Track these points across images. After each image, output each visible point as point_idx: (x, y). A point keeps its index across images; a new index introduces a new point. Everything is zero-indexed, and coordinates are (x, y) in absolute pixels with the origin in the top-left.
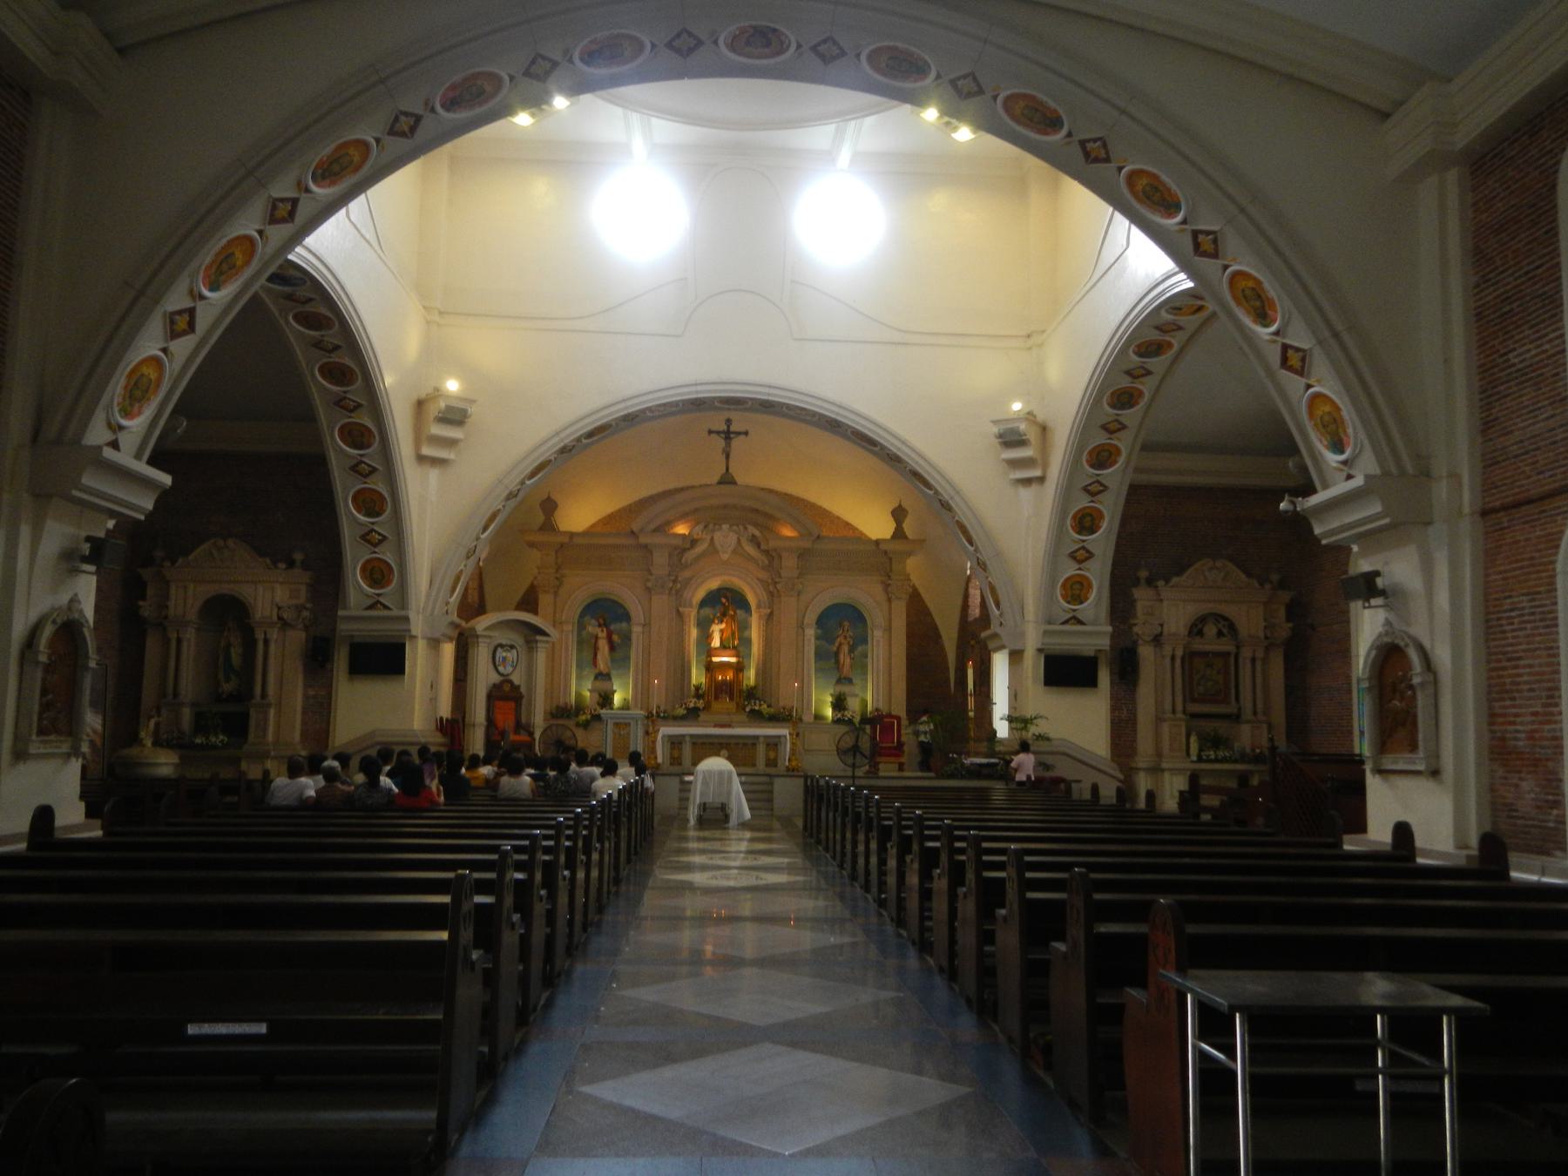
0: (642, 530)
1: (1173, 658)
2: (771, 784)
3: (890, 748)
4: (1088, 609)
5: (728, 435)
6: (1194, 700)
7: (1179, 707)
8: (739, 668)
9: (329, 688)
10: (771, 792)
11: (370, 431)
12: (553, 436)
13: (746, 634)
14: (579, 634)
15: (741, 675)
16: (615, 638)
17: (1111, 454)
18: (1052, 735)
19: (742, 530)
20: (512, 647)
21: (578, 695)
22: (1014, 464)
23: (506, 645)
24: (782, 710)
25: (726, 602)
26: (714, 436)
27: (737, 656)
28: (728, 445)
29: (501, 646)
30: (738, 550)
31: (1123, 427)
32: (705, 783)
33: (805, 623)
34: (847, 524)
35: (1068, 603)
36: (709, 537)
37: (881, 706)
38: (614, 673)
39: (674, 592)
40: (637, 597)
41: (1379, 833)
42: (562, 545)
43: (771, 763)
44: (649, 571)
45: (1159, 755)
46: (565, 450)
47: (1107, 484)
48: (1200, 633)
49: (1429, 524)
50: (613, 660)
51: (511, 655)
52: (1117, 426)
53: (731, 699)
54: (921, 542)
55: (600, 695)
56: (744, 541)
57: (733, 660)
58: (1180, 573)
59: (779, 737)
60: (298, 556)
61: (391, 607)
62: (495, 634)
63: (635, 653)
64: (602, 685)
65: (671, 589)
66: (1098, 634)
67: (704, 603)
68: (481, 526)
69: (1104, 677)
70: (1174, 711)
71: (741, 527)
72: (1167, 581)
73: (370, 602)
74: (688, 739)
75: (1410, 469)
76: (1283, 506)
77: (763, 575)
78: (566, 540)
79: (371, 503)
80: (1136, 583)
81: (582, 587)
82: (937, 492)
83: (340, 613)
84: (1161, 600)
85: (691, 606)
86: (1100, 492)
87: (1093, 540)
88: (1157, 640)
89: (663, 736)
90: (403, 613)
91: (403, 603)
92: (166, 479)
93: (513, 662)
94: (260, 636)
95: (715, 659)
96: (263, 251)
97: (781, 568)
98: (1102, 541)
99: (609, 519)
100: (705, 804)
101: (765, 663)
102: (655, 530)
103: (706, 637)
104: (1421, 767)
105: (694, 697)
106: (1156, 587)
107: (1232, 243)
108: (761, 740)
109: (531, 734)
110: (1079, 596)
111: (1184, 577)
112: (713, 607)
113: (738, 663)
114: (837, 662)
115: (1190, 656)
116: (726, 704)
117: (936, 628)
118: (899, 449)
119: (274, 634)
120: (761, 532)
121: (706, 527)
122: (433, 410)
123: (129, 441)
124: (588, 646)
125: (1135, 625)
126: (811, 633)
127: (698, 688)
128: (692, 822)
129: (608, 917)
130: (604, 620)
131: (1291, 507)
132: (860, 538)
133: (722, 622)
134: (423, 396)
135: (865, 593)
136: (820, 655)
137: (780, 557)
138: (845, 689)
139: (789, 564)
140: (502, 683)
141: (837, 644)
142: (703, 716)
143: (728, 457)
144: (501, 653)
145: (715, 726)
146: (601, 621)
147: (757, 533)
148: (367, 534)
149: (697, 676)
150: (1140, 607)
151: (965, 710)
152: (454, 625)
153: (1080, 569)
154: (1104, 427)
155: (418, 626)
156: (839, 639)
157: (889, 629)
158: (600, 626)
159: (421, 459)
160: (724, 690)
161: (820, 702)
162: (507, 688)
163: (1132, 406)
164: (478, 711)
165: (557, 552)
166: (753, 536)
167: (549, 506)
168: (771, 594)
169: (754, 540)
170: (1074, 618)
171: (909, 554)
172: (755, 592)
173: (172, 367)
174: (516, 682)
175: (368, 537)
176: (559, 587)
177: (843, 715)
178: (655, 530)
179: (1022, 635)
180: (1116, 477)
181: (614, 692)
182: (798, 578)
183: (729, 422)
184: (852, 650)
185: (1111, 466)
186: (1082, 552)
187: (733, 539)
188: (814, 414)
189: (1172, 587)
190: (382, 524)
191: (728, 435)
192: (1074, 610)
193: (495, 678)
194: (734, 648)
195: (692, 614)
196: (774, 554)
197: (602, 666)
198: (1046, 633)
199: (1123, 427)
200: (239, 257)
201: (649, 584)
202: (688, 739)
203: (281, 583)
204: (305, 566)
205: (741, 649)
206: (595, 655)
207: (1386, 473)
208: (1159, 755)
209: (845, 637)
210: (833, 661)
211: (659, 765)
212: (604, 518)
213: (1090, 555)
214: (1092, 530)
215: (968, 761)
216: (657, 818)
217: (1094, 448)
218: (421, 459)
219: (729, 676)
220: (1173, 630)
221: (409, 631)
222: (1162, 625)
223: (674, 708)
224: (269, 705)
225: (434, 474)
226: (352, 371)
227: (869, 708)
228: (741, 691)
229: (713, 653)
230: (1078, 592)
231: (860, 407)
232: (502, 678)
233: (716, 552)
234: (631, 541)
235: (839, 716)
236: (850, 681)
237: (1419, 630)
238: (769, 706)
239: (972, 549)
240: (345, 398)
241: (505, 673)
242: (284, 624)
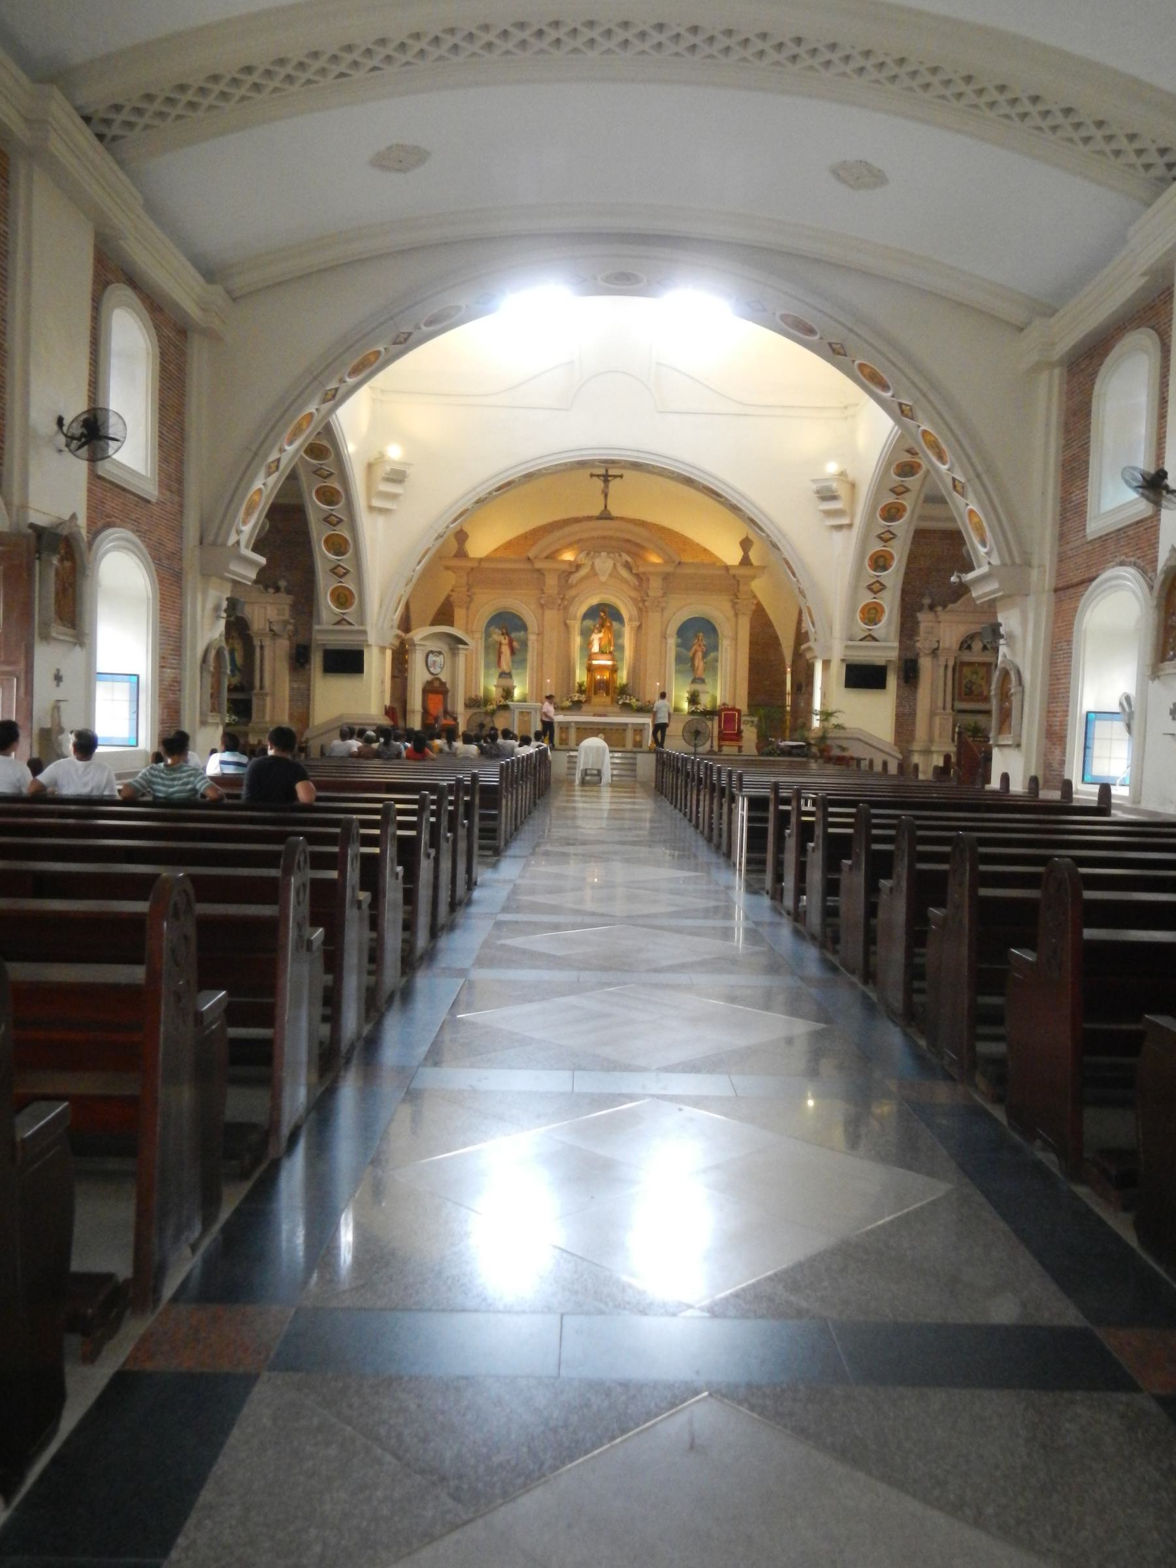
0: (536, 558)
1: (946, 667)
2: (635, 758)
3: (731, 734)
4: (879, 629)
5: (606, 478)
6: (961, 700)
7: (949, 706)
8: (614, 670)
9: (308, 682)
10: (635, 764)
11: (338, 492)
12: (471, 491)
13: (620, 641)
14: (486, 640)
15: (615, 676)
16: (515, 644)
17: (898, 510)
18: (847, 725)
20: (440, 653)
21: (486, 690)
22: (829, 514)
24: (648, 704)
25: (604, 615)
26: (595, 479)
27: (613, 660)
28: (607, 486)
29: (432, 652)
30: (614, 574)
31: (907, 490)
32: (586, 755)
33: (668, 632)
34: (705, 550)
35: (866, 624)
36: (590, 563)
37: (727, 702)
38: (514, 672)
39: (562, 607)
41: (995, 784)
42: (472, 569)
43: (638, 744)
44: (542, 590)
45: (931, 740)
46: (480, 502)
47: (895, 532)
48: (969, 648)
49: (1027, 595)
50: (513, 662)
52: (903, 489)
53: (607, 694)
54: (764, 568)
55: (503, 690)
56: (618, 565)
57: (609, 663)
58: (954, 601)
59: (644, 724)
60: (282, 584)
61: (351, 621)
62: (428, 643)
63: (531, 656)
64: (505, 682)
65: (560, 605)
66: (892, 648)
67: (586, 616)
68: (417, 561)
69: (892, 681)
70: (944, 708)
71: (617, 555)
72: (945, 607)
73: (337, 619)
74: (573, 725)
75: (1018, 560)
76: (953, 579)
77: (634, 594)
78: (476, 565)
79: (338, 546)
80: (921, 608)
81: (488, 603)
82: (768, 536)
83: (316, 627)
84: (939, 622)
85: (575, 619)
86: (891, 539)
87: (885, 576)
88: (934, 653)
90: (361, 628)
91: (362, 622)
92: (263, 560)
94: (257, 643)
95: (595, 662)
96: (317, 417)
97: (648, 588)
98: (893, 577)
99: (509, 545)
100: (586, 770)
101: (634, 667)
102: (547, 558)
103: (587, 644)
104: (1010, 742)
105: (578, 693)
106: (936, 612)
107: (919, 414)
108: (630, 726)
109: (455, 719)
110: (874, 619)
111: (959, 602)
112: (594, 619)
113: (613, 665)
114: (693, 666)
115: (959, 666)
116: (602, 699)
117: (777, 638)
118: (739, 501)
119: (267, 642)
120: (632, 558)
121: (588, 554)
122: (380, 472)
123: (244, 539)
124: (493, 651)
125: (918, 641)
126: (672, 641)
127: (581, 685)
128: (577, 782)
129: (533, 815)
130: (507, 630)
131: (958, 580)
132: (715, 563)
133: (600, 632)
134: (372, 460)
135: (717, 609)
136: (679, 659)
137: (648, 579)
138: (698, 687)
139: (655, 585)
141: (693, 651)
142: (585, 708)
143: (606, 496)
144: (431, 658)
145: (594, 715)
146: (504, 631)
147: (629, 559)
148: (335, 568)
149: (581, 676)
150: (923, 627)
151: (784, 706)
152: (398, 637)
153: (875, 598)
154: (893, 491)
155: (373, 638)
156: (695, 647)
157: (735, 639)
158: (503, 634)
159: (371, 509)
160: (603, 687)
161: (678, 697)
162: (437, 684)
163: (913, 475)
164: (416, 701)
165: (468, 574)
166: (627, 562)
167: (461, 536)
168: (640, 610)
169: (627, 566)
170: (870, 636)
171: (753, 577)
173: (266, 492)
174: (444, 680)
175: (336, 571)
176: (471, 600)
177: (696, 708)
178: (547, 558)
179: (830, 649)
180: (903, 527)
181: (514, 687)
182: (662, 597)
183: (607, 471)
184: (705, 655)
185: (898, 520)
186: (878, 584)
187: (609, 564)
188: (673, 472)
189: (949, 611)
190: (346, 561)
191: (606, 478)
192: (870, 630)
193: (429, 677)
194: (611, 653)
195: (576, 626)
196: (643, 578)
197: (505, 666)
198: (847, 647)
199: (907, 490)
200: (305, 424)
201: (542, 601)
202: (573, 725)
203: (271, 604)
204: (289, 592)
205: (615, 654)
206: (500, 657)
207: (1004, 565)
208: (931, 740)
209: (700, 646)
210: (689, 664)
212: (504, 544)
213: (883, 587)
214: (885, 568)
215: (783, 744)
216: (552, 780)
217: (886, 506)
218: (371, 509)
219: (606, 676)
220: (947, 646)
221: (367, 641)
222: (938, 642)
223: (562, 701)
224: (266, 694)
225: (381, 520)
226: (327, 450)
227: (719, 703)
228: (615, 688)
229: (593, 657)
230: (873, 616)
231: (707, 467)
232: (433, 677)
233: (596, 574)
234: (529, 566)
235: (693, 709)
236: (702, 681)
237: (1018, 661)
238: (637, 700)
239: (795, 580)
240: (321, 469)
242: (274, 635)
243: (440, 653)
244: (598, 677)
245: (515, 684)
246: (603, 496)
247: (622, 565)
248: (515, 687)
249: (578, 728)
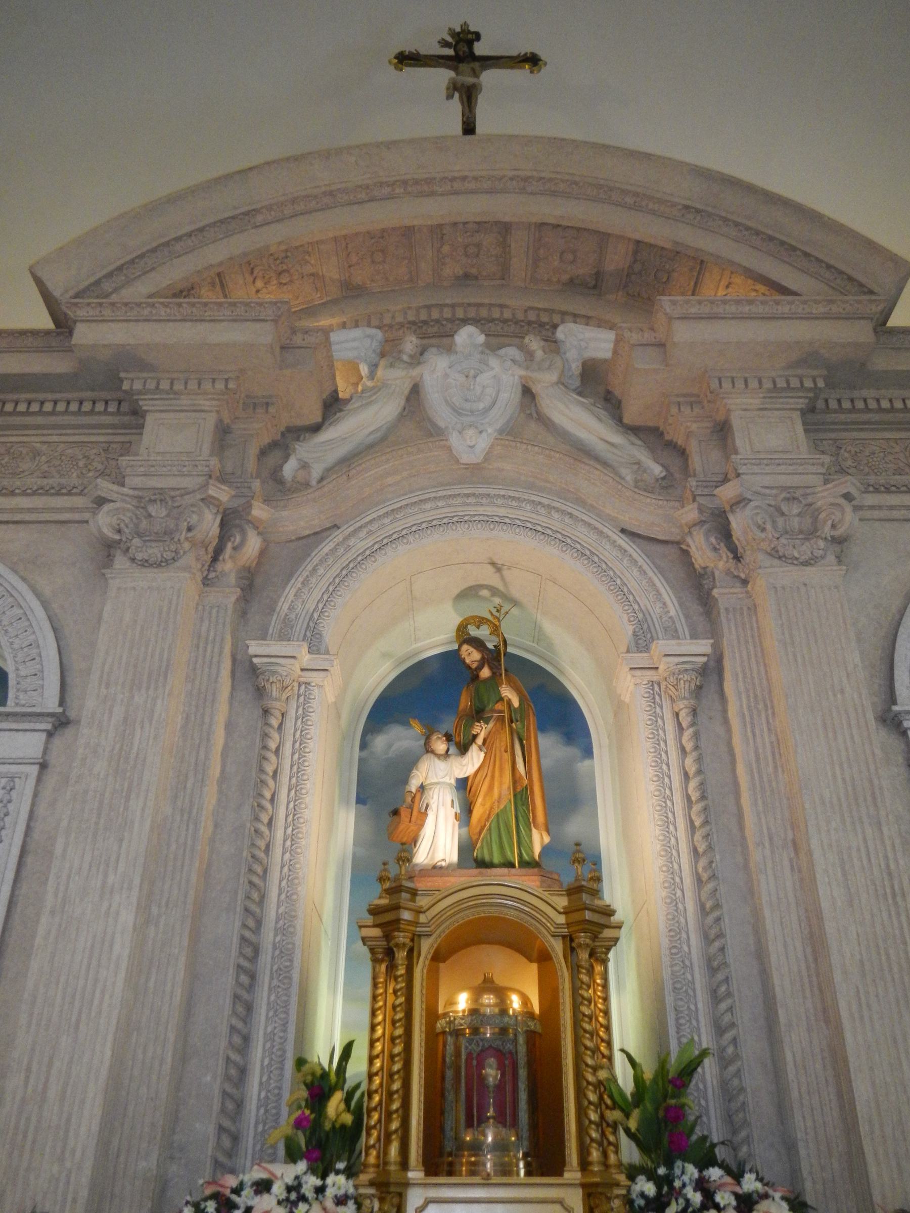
13: (574, 829)
19: (539, 354)
40: (45, 605)
71: (534, 343)
105: (292, 1156)
121: (383, 355)
133: (463, 749)
172: (622, 592)
194: (528, 864)
228: (606, 1087)
244: (463, 1002)
246: (455, 106)
247: (560, 382)
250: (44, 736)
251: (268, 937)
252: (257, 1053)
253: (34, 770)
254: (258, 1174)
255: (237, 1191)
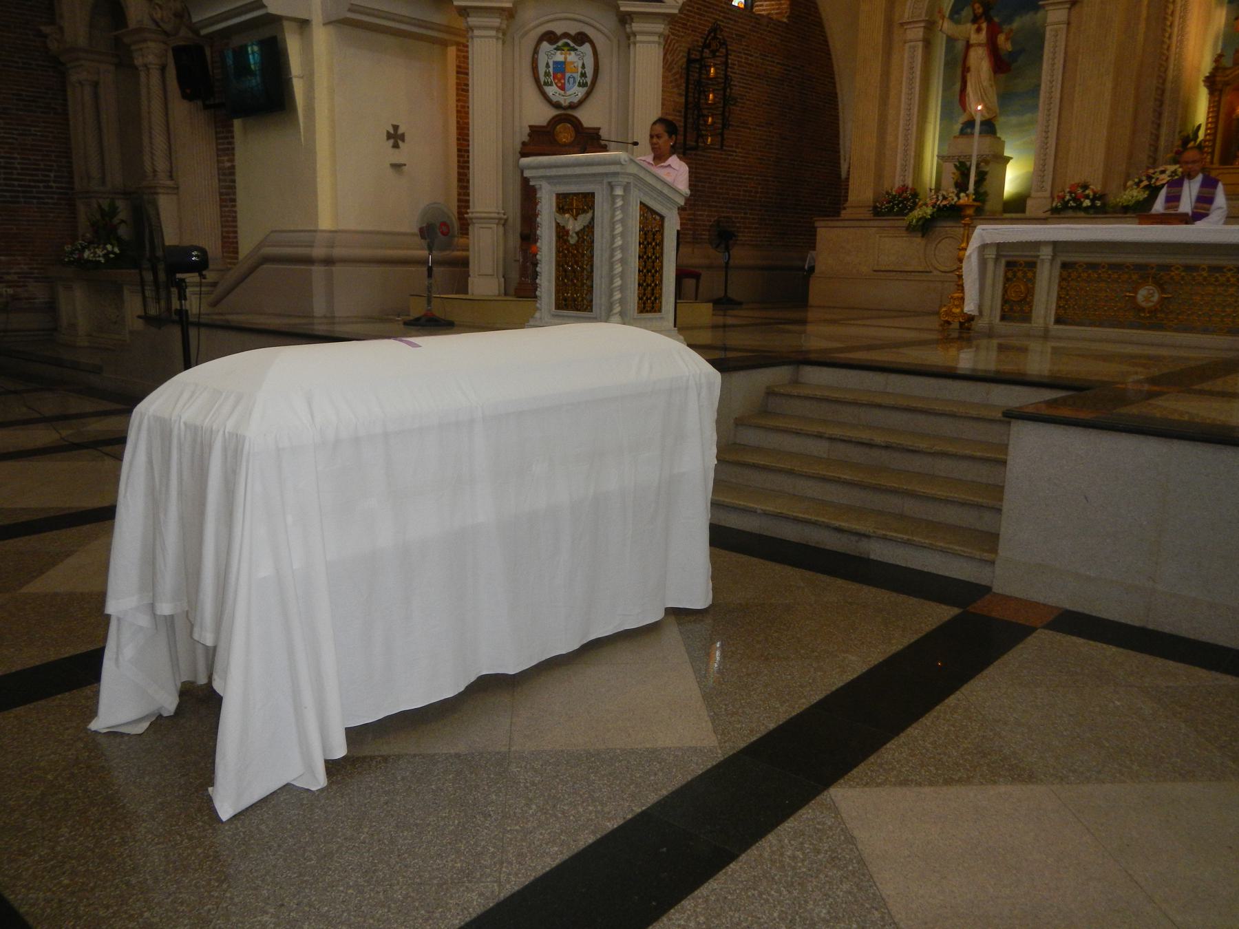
20: (581, 38)
23: (566, 35)
29: (550, 37)
51: (579, 59)
64: (976, 146)
74: (1046, 253)
89: (983, 247)
93: (583, 75)
140: (555, 121)
144: (549, 55)
158: (975, 20)
211: (971, 318)
232: (554, 112)
241: (564, 101)
243: (581, 38)
245: (1007, 153)
248: (1008, 159)
249: (1065, 266)
250: (1066, 11)
251: (1169, 86)
252: (1164, 130)
253: (1065, 26)
254: (1161, 168)
255: (1154, 173)
